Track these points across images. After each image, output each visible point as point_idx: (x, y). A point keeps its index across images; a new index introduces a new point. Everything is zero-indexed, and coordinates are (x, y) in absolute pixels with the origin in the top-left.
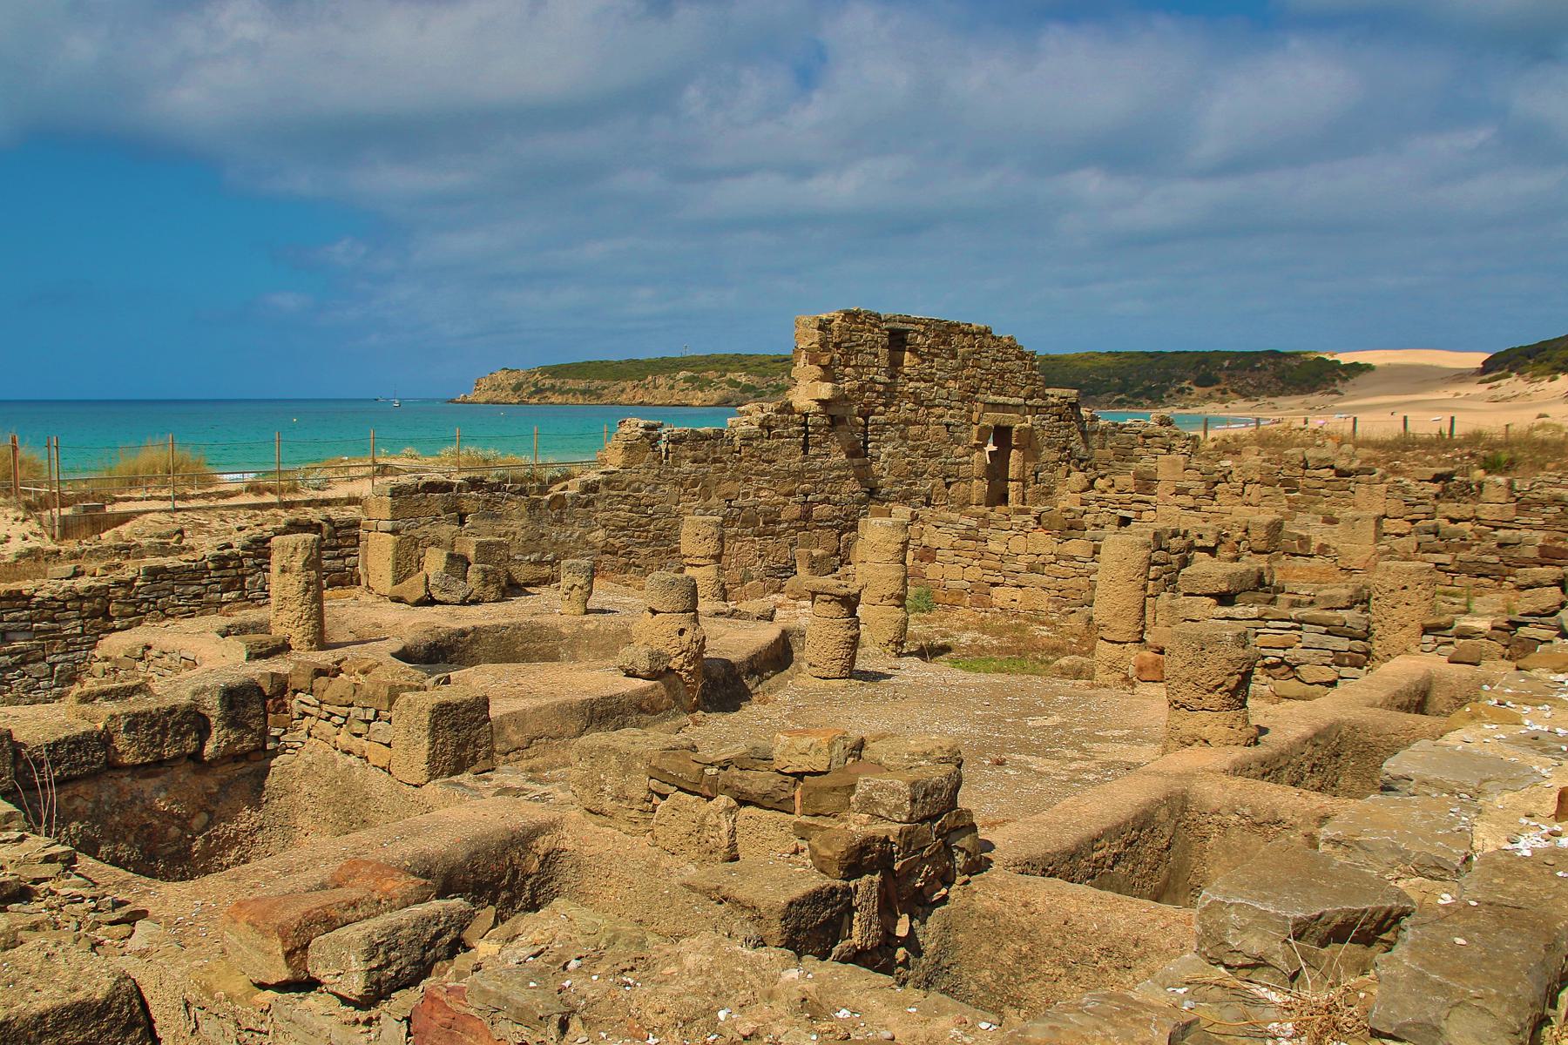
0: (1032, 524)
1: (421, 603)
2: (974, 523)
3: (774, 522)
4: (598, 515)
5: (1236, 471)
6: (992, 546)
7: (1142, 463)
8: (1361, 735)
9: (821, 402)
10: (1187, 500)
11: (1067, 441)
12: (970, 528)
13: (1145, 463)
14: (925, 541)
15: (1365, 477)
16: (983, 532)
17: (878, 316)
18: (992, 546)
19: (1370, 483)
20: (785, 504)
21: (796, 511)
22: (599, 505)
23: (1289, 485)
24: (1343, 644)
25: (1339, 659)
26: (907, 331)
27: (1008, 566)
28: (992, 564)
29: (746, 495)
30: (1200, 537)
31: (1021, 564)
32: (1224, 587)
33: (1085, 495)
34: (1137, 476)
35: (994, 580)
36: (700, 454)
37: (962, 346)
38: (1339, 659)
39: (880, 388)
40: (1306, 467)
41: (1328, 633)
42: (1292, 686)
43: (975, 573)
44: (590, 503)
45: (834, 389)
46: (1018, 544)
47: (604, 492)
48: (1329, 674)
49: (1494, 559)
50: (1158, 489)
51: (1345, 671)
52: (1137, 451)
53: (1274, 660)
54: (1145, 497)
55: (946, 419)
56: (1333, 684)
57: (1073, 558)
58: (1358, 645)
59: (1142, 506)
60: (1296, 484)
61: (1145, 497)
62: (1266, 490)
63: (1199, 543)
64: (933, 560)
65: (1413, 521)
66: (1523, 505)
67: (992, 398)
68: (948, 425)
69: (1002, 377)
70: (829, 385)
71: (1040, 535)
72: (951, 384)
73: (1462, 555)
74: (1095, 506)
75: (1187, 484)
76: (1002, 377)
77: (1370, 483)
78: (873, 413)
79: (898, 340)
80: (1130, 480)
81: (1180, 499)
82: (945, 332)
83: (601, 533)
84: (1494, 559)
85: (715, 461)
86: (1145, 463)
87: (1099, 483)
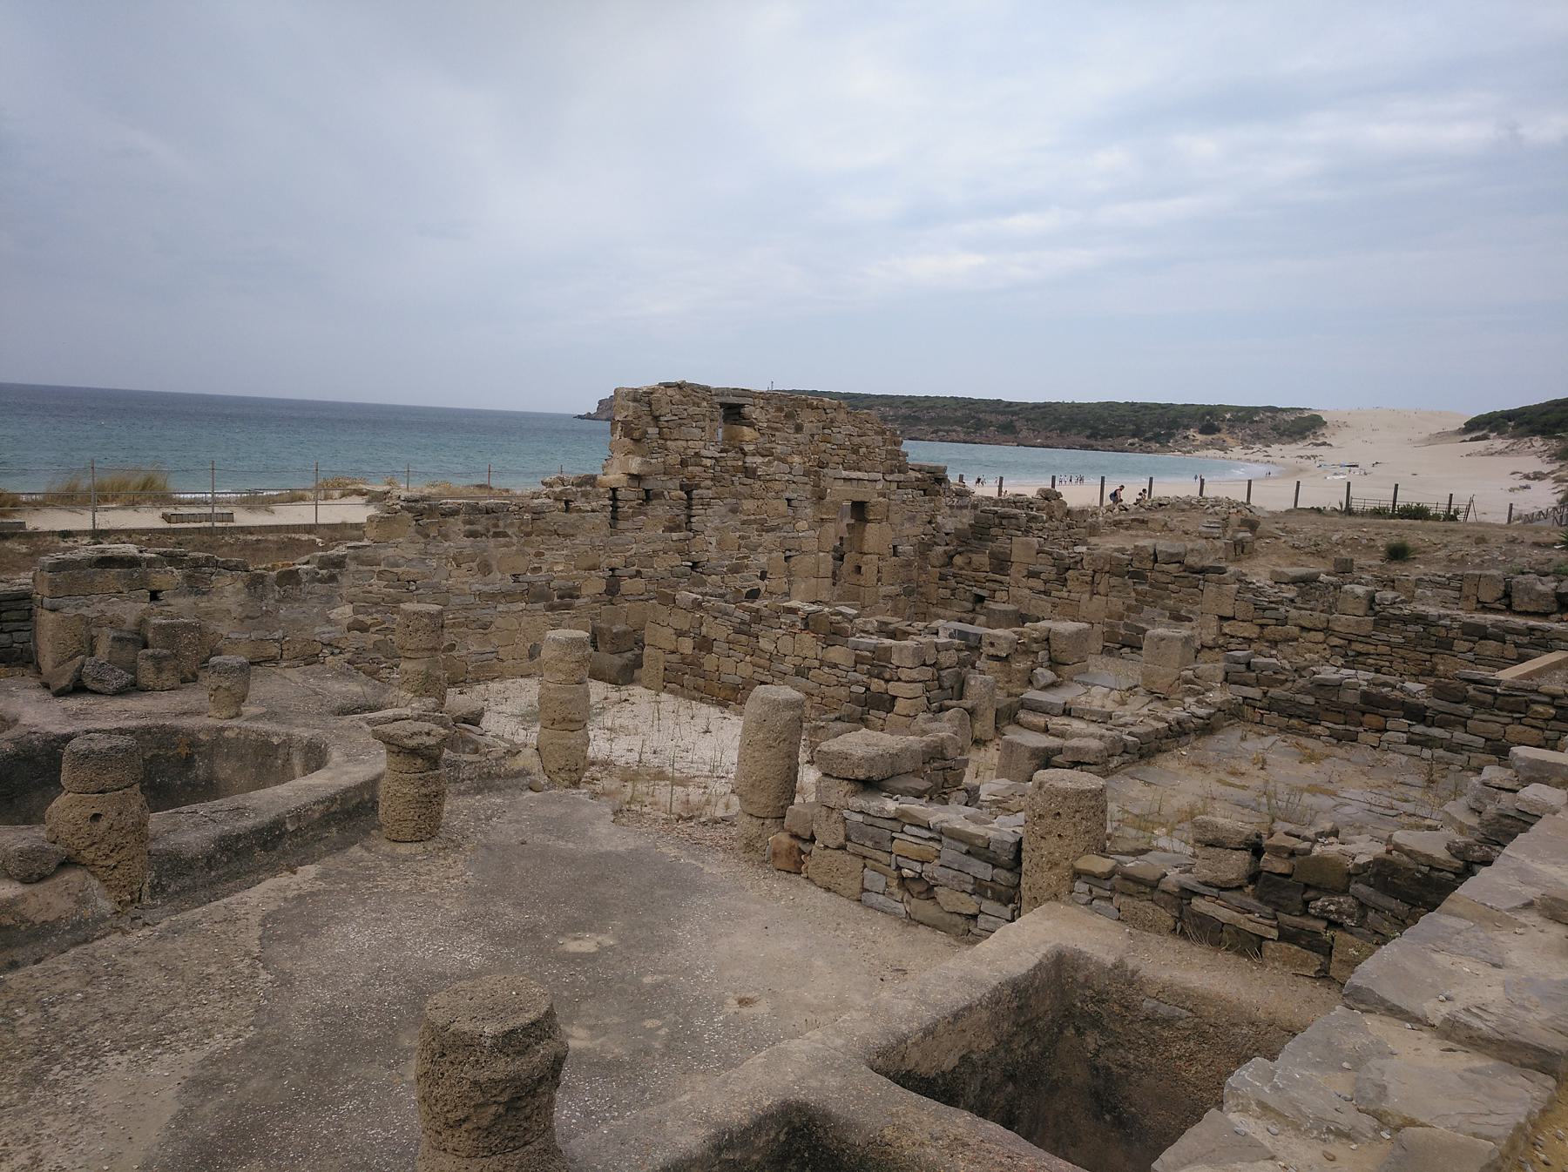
0: (800, 625)
1: (61, 693)
2: (747, 617)
3: (571, 597)
4: (344, 592)
5: (1087, 559)
6: (763, 643)
7: (998, 543)
8: (821, 1132)
9: (633, 477)
10: (1037, 584)
11: (933, 516)
12: (743, 622)
13: (1001, 543)
14: (704, 630)
15: (1214, 577)
16: (755, 628)
17: (707, 389)
18: (763, 643)
19: (1220, 583)
20: (586, 579)
21: (601, 586)
22: (343, 580)
23: (1138, 576)
24: (984, 871)
25: (980, 888)
26: (743, 406)
27: (777, 666)
28: (762, 662)
29: (536, 570)
30: (992, 644)
31: (788, 666)
32: (861, 774)
33: (944, 571)
34: (992, 555)
35: (763, 678)
36: (478, 528)
37: (809, 420)
38: (980, 888)
39: (708, 462)
40: (1156, 561)
41: (968, 853)
42: (925, 909)
43: (746, 670)
44: (332, 578)
45: (642, 463)
46: (786, 644)
47: (352, 566)
48: (969, 905)
49: (1310, 700)
50: (1012, 571)
51: (988, 905)
52: (994, 531)
53: (911, 874)
54: (998, 577)
55: (787, 495)
56: (974, 917)
57: (835, 666)
58: (1004, 876)
59: (996, 586)
60: (1145, 578)
61: (998, 577)
62: (1115, 581)
63: (992, 651)
64: (710, 651)
65: (1262, 626)
66: (1383, 622)
67: (845, 474)
68: (789, 500)
69: (856, 452)
70: (638, 460)
71: (807, 638)
72: (797, 459)
73: (1273, 692)
74: (952, 582)
75: (1039, 568)
76: (856, 452)
77: (1220, 583)
78: (698, 487)
79: (733, 409)
80: (986, 560)
81: (1033, 582)
82: (791, 405)
83: (347, 610)
84: (1310, 700)
85: (496, 535)
86: (1001, 543)
87: (958, 560)
